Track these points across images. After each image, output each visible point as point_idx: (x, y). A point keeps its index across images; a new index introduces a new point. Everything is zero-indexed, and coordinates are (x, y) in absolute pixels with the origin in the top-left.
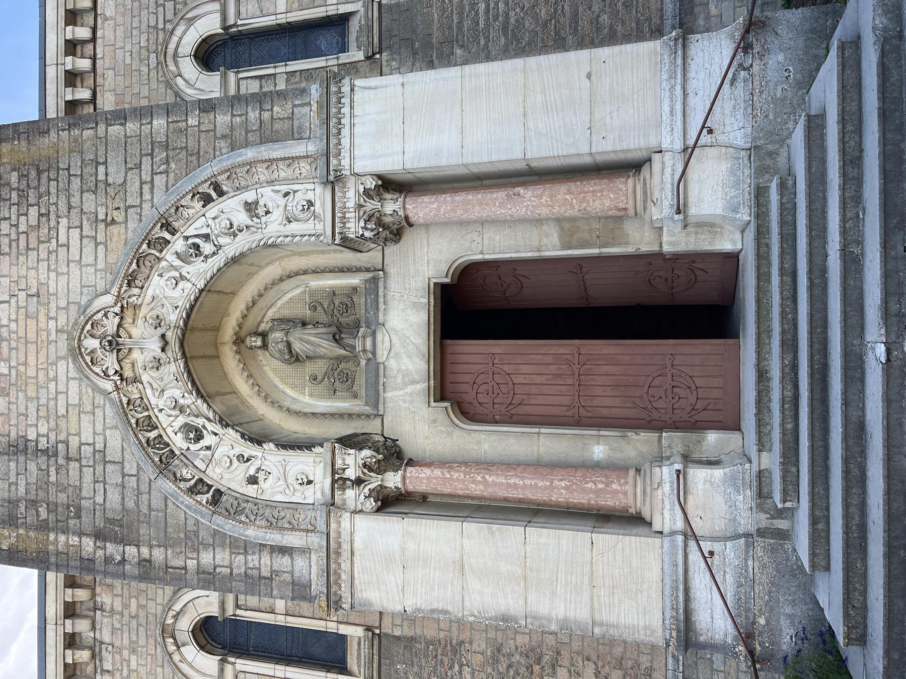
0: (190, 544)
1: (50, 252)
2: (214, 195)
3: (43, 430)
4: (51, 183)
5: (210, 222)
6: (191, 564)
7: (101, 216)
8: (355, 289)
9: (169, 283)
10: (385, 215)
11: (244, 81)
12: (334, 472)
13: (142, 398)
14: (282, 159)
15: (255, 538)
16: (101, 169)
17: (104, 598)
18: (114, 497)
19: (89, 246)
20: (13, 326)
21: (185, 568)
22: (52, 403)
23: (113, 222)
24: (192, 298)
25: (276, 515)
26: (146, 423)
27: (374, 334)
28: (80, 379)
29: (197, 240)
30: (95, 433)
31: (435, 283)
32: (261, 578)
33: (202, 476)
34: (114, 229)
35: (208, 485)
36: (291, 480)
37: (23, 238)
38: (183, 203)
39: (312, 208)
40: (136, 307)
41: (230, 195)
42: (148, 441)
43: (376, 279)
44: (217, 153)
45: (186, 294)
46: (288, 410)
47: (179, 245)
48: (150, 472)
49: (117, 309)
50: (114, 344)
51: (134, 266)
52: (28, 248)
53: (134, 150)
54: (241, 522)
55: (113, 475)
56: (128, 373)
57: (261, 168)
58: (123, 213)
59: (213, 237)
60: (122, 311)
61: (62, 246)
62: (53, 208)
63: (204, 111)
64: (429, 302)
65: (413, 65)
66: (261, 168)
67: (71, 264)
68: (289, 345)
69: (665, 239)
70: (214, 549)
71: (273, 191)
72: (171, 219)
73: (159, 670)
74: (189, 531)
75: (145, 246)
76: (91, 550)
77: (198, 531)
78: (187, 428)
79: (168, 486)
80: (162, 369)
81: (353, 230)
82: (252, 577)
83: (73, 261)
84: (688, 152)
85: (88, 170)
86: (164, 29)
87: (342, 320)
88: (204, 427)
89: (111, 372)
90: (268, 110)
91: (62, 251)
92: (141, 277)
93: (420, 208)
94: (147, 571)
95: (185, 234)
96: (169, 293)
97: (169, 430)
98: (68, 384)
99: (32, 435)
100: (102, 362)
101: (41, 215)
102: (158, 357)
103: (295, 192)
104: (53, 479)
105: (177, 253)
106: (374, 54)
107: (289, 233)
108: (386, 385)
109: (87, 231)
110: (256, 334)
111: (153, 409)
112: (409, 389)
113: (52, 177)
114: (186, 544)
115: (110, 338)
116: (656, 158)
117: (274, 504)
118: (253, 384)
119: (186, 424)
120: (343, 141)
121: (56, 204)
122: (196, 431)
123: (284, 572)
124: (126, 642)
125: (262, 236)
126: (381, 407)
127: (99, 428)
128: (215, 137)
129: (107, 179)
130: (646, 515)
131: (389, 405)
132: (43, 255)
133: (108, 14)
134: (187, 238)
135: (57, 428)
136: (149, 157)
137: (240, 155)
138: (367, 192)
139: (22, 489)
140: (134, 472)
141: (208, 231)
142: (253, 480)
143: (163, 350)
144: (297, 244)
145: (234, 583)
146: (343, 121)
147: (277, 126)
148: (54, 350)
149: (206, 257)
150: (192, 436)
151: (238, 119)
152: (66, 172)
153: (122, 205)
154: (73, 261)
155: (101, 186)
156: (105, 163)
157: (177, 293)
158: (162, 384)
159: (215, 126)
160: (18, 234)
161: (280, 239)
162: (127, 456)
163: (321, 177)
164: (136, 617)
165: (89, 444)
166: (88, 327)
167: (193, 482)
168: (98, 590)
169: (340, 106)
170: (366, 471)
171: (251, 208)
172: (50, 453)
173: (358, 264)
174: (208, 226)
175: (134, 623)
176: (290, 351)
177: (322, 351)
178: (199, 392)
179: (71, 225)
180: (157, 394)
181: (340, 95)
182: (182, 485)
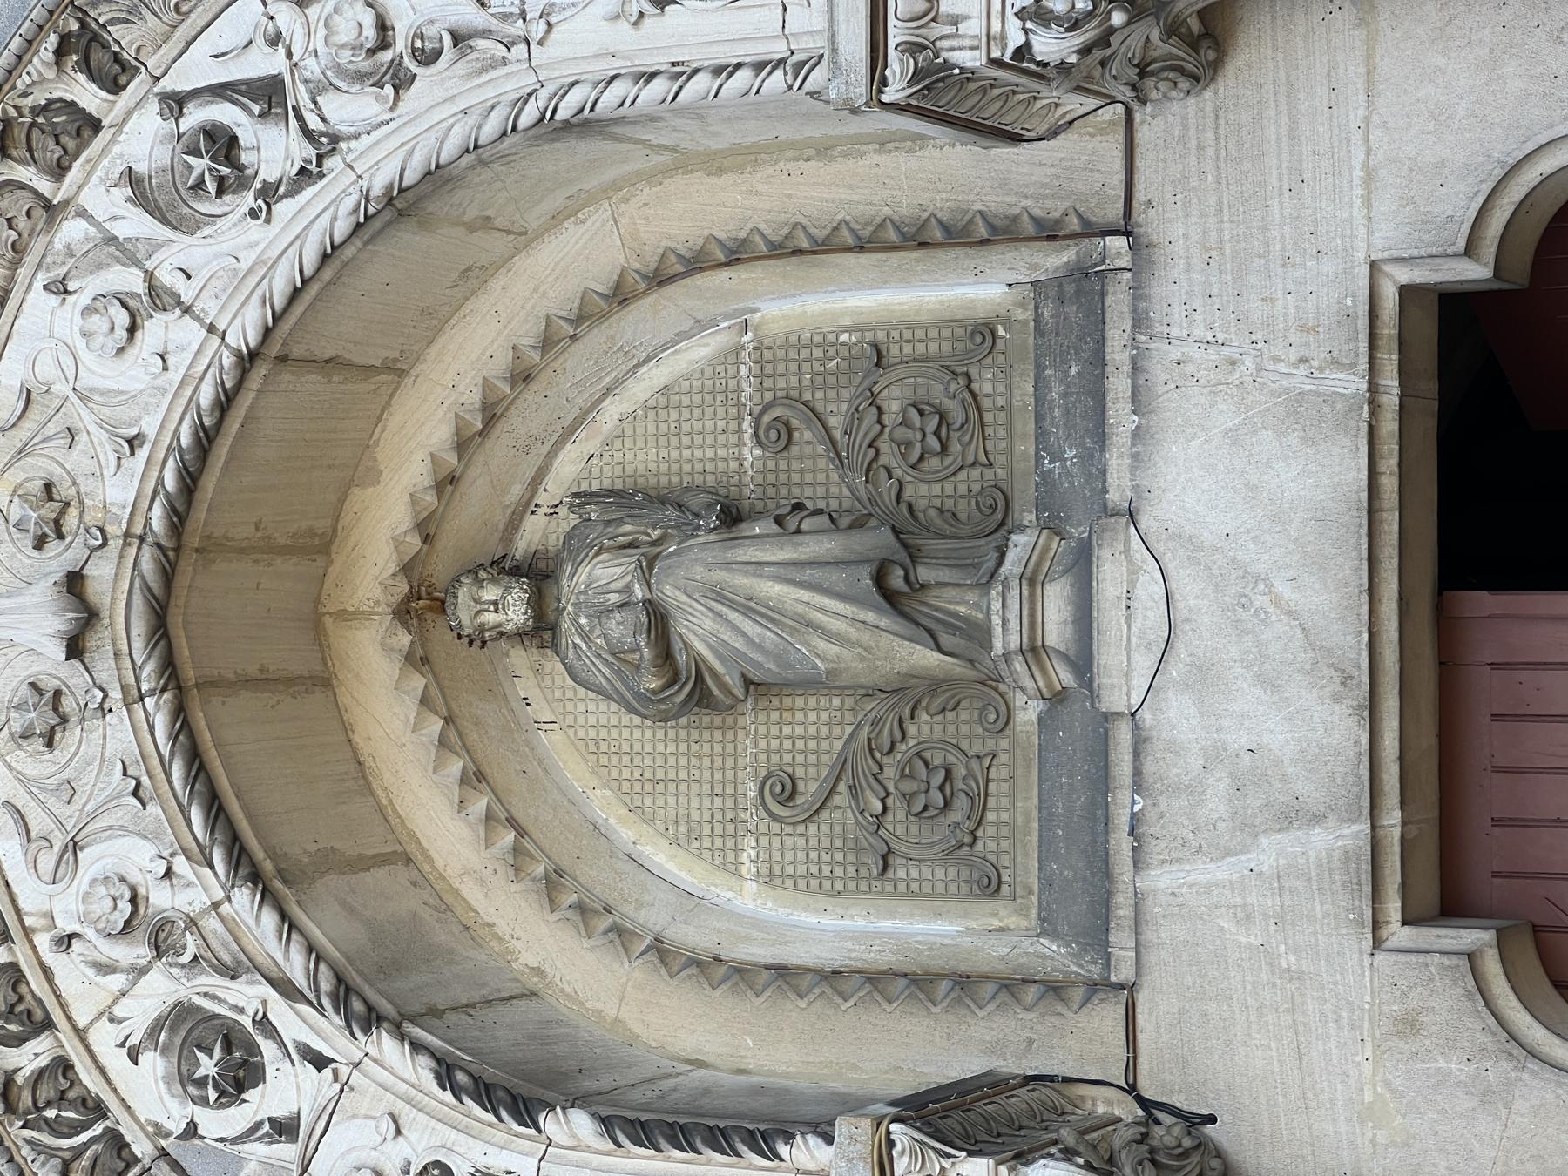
8: (983, 332)
9: (98, 323)
24: (206, 395)
27: (1082, 565)
29: (225, 113)
31: (1408, 293)
45: (175, 376)
47: (140, 136)
59: (298, 95)
64: (1373, 388)
68: (658, 621)
72: (103, 14)
80: (69, 739)
87: (920, 492)
88: (263, 1023)
95: (167, 85)
96: (100, 371)
97: (104, 1039)
102: (50, 684)
105: (131, 178)
107: (660, 61)
110: (505, 568)
111: (27, 933)
112: (1269, 852)
118: (489, 817)
122: (228, 1046)
131: (1164, 933)
134: (176, 103)
143: (75, 649)
144: (694, 112)
149: (269, 193)
150: (208, 1066)
157: (133, 373)
161: (618, 90)
173: (1000, 202)
180: (47, 861)
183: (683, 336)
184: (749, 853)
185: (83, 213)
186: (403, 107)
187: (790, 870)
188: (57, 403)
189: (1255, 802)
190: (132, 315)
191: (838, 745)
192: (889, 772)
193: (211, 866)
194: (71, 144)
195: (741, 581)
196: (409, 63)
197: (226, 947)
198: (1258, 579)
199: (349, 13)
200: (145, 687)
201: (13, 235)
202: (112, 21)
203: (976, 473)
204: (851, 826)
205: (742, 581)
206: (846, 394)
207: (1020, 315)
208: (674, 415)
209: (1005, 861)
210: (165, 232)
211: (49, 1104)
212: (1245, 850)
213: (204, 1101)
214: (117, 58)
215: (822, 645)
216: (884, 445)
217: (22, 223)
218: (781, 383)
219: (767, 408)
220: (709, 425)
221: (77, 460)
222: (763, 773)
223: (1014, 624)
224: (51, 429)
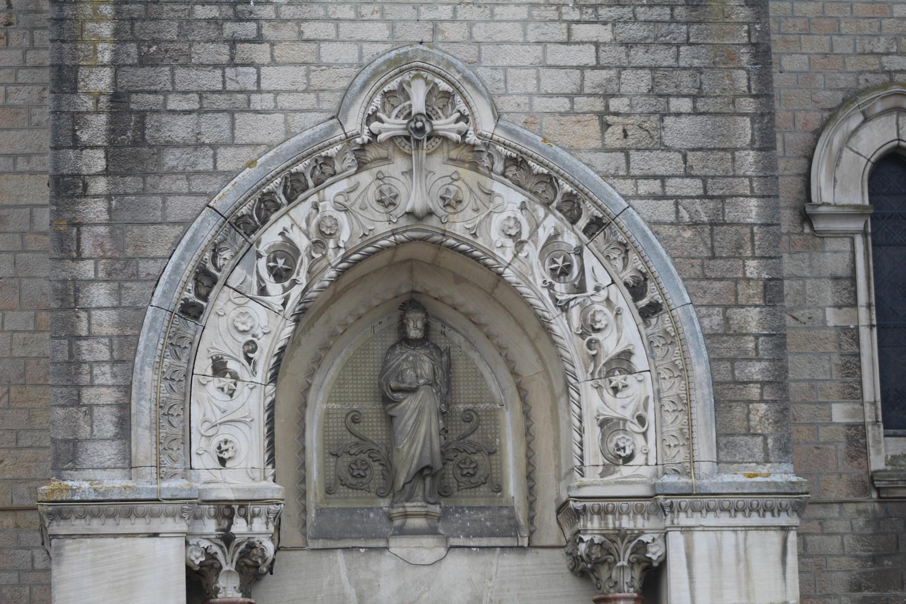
0: (118, 266)
2: (643, 303)
4: (667, 11)
5: (603, 293)
6: (87, 269)
7: (615, 104)
8: (499, 489)
9: (512, 223)
10: (610, 569)
11: (848, 247)
12: (243, 503)
13: (335, 174)
14: (690, 420)
15: (140, 382)
16: (685, 105)
18: (180, 129)
19: (567, 81)
21: (80, 258)
22: (321, 12)
23: (605, 126)
24: (490, 261)
25: (174, 411)
26: (297, 185)
27: (432, 532)
28: (362, 67)
29: (575, 270)
30: (277, 93)
32: (79, 387)
33: (220, 283)
34: (594, 125)
35: (208, 294)
36: (225, 432)
38: (633, 256)
39: (621, 461)
40: (475, 166)
41: (642, 327)
42: (270, 193)
44: (703, 311)
45: (495, 251)
46: (307, 390)
47: (570, 239)
48: (227, 197)
49: (472, 138)
50: (417, 136)
51: (538, 168)
53: (713, 165)
54: (162, 357)
55: (214, 128)
56: (372, 153)
57: (678, 387)
58: (618, 144)
59: (581, 298)
60: (468, 145)
61: (569, 30)
62: (627, 12)
63: (765, 286)
65: (857, 557)
66: (678, 387)
67: (540, 48)
68: (412, 391)
70: (114, 308)
71: (647, 398)
72: (607, 231)
74: (138, 263)
75: (567, 188)
76: (92, 86)
77: (138, 280)
79: (206, 228)
80: (381, 209)
81: (589, 526)
82: (78, 374)
83: (544, 52)
85: (686, 81)
87: (450, 466)
88: (294, 283)
89: (375, 126)
90: (761, 394)
91: (558, 32)
92: (521, 176)
94: (67, 188)
95: (586, 249)
96: (497, 220)
97: (285, 222)
98: (351, 42)
100: (388, 107)
102: (397, 201)
103: (644, 434)
104: (202, 12)
105: (557, 235)
106: (878, 490)
107: (585, 424)
108: (355, 554)
110: (427, 327)
111: (318, 192)
113: (677, 11)
114: (118, 259)
115: (428, 129)
117: (187, 405)
118: (346, 324)
119: (297, 252)
120: (711, 515)
121: (635, 19)
122: (287, 270)
123: (91, 426)
125: (581, 378)
126: (320, 544)
127: (285, 101)
128: (726, 308)
129: (670, 114)
131: (324, 558)
134: (579, 252)
135: (279, 20)
136: (701, 192)
137: (698, 353)
140: (221, 166)
141: (590, 290)
142: (219, 368)
143: (410, 214)
145: (66, 342)
146: (740, 515)
147: (738, 411)
148: (406, 16)
149: (551, 287)
150: (281, 262)
151: (751, 345)
152: (682, 38)
153: (631, 141)
154: (544, 52)
155: (661, 104)
156: (695, 112)
157: (496, 236)
158: (356, 208)
159: (742, 307)
162: (245, 154)
163: (663, 485)
165: (258, 82)
166: (444, 86)
167: (213, 270)
169: (761, 512)
170: (243, 547)
171: (623, 360)
174: (597, 289)
176: (400, 390)
177: (403, 445)
178: (344, 271)
179: (602, 48)
180: (341, 199)
181: (776, 511)
182: (208, 255)
183: (499, 384)
184: (336, 406)
185: (546, 216)
186: (575, 336)
187: (330, 421)
188: (487, 204)
189: (364, 587)
190: (515, 236)
191: (370, 438)
192: (362, 456)
193: (341, 262)
194: (568, 214)
195: (425, 418)
196: (589, 338)
197: (318, 269)
198: (429, 587)
199: (604, 318)
200: (397, 236)
201: (540, 192)
202: (605, 233)
203: (456, 485)
204: (345, 442)
205: (425, 418)
206: (480, 440)
207: (504, 500)
208: (474, 379)
209: (337, 495)
210: (539, 248)
211: (265, 206)
212: (350, 584)
213: (268, 261)
214: (593, 234)
215: (407, 447)
216: (464, 454)
217: (544, 195)
218: (484, 418)
219: (476, 413)
220: (470, 392)
221: (469, 213)
222: (361, 411)
223: (414, 509)
224: (479, 202)
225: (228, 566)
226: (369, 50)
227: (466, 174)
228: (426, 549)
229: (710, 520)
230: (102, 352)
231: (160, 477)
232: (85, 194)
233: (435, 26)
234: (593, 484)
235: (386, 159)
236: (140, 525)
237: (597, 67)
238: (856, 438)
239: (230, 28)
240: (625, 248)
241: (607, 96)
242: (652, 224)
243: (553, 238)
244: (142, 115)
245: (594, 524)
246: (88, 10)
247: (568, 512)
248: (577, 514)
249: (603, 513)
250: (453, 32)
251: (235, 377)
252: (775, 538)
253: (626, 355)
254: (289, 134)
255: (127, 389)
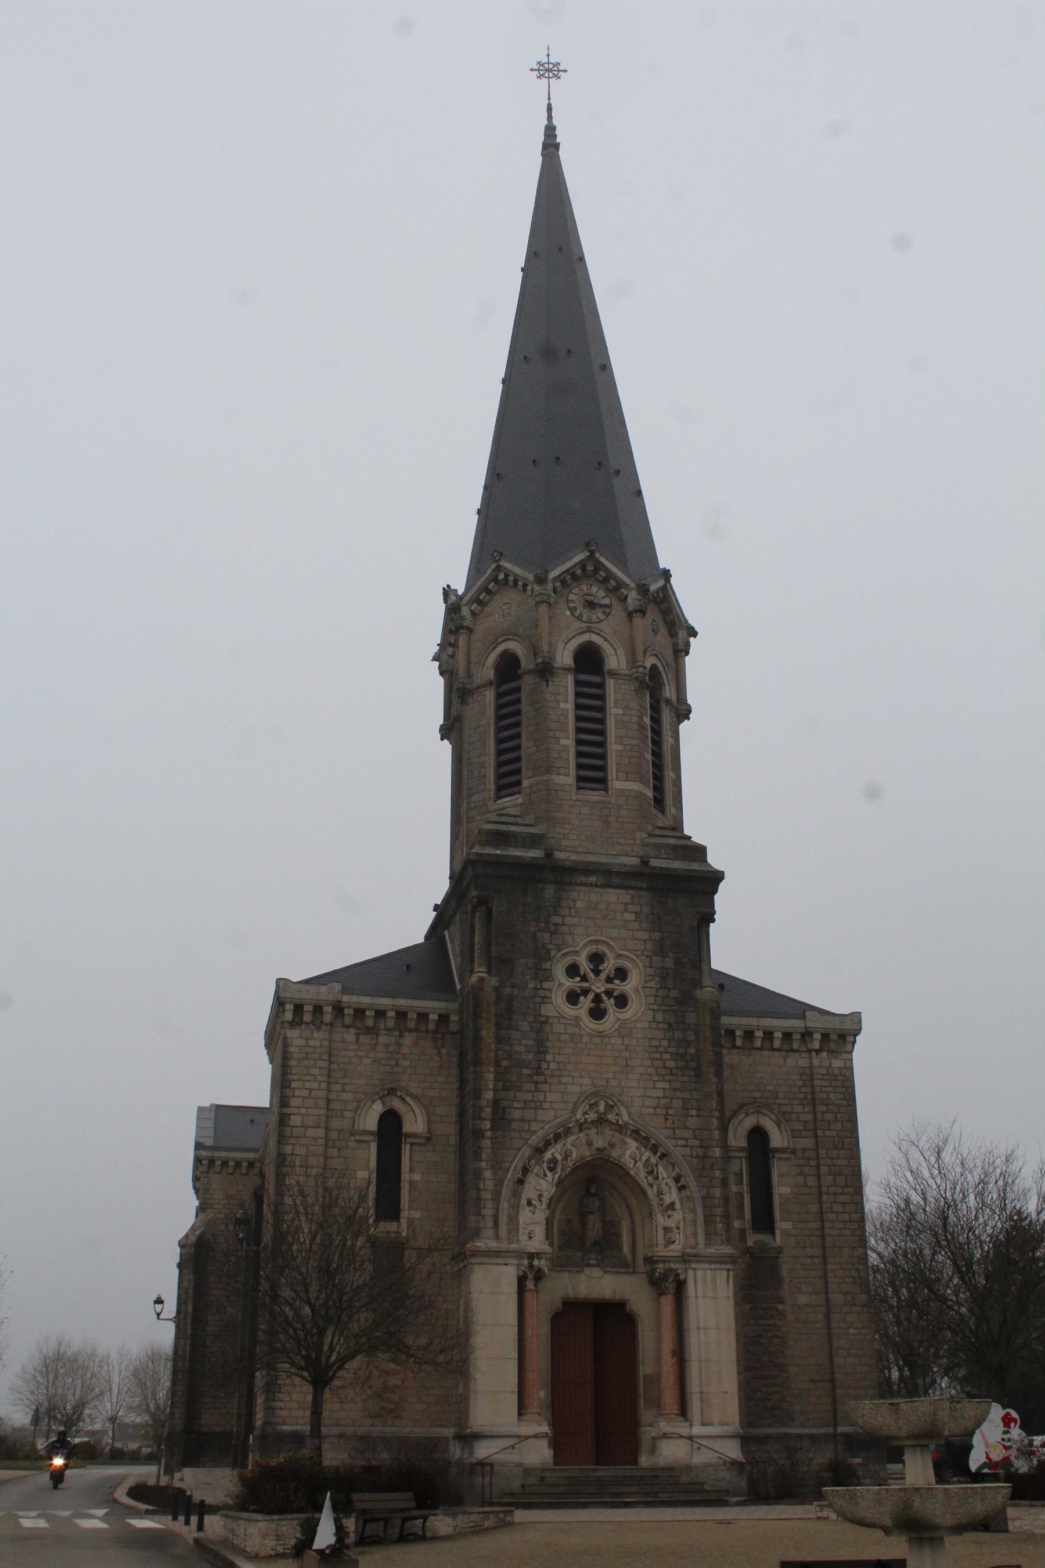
1: (650, 1075)
3: (553, 1066)
6: (484, 1164)
7: (670, 1111)
8: (620, 1249)
16: (694, 1113)
17: (408, 1039)
18: (517, 1114)
19: (653, 1103)
20: (609, 1047)
21: (481, 1160)
25: (513, 1219)
27: (598, 1266)
30: (552, 1102)
34: (663, 1119)
36: (531, 1227)
37: (657, 1056)
40: (620, 1132)
43: (626, 1267)
47: (653, 1160)
48: (534, 1140)
49: (620, 1122)
52: (653, 1059)
55: (529, 1114)
56: (585, 1126)
62: (674, 1078)
68: (592, 1213)
69: (648, 1428)
73: (363, 1081)
78: (554, 1161)
79: (526, 1152)
84: (690, 1438)
86: (775, 1104)
91: (650, 1084)
93: (667, 1302)
96: (628, 1152)
97: (553, 1150)
99: (549, 1057)
101: (671, 1069)
104: (525, 1071)
109: (663, 1101)
116: (687, 1424)
124: (381, 1055)
127: (555, 1106)
130: (525, 1418)
132: (650, 1070)
133: (788, 1060)
134: (657, 1165)
135: (552, 1076)
138: (678, 1275)
139: (517, 1048)
140: (532, 1129)
142: (529, 1203)
143: (598, 1149)
156: (698, 1116)
160: (661, 1053)
164: (397, 1065)
166: (611, 1103)
168: (414, 1034)
172: (538, 1071)
175: (393, 1062)
225: (531, 1276)
226: (584, 1088)
227: (617, 1135)
228: (596, 1272)
229: (703, 1266)
230: (489, 1196)
231: (509, 1243)
232: (483, 1137)
233: (607, 1079)
234: (661, 1251)
235: (589, 1129)
236: (501, 1261)
237: (664, 1097)
238: (742, 1233)
239: (535, 1078)
240: (673, 1165)
241: (668, 1108)
242: (683, 1156)
243: (647, 1160)
244: (504, 1109)
245: (661, 1266)
246: (485, 1069)
247: (649, 1260)
248: (656, 1262)
249: (664, 1262)
250: (614, 1083)
251: (535, 1207)
252: (725, 1273)
253: (673, 1204)
254: (556, 1118)
255: (497, 1209)
